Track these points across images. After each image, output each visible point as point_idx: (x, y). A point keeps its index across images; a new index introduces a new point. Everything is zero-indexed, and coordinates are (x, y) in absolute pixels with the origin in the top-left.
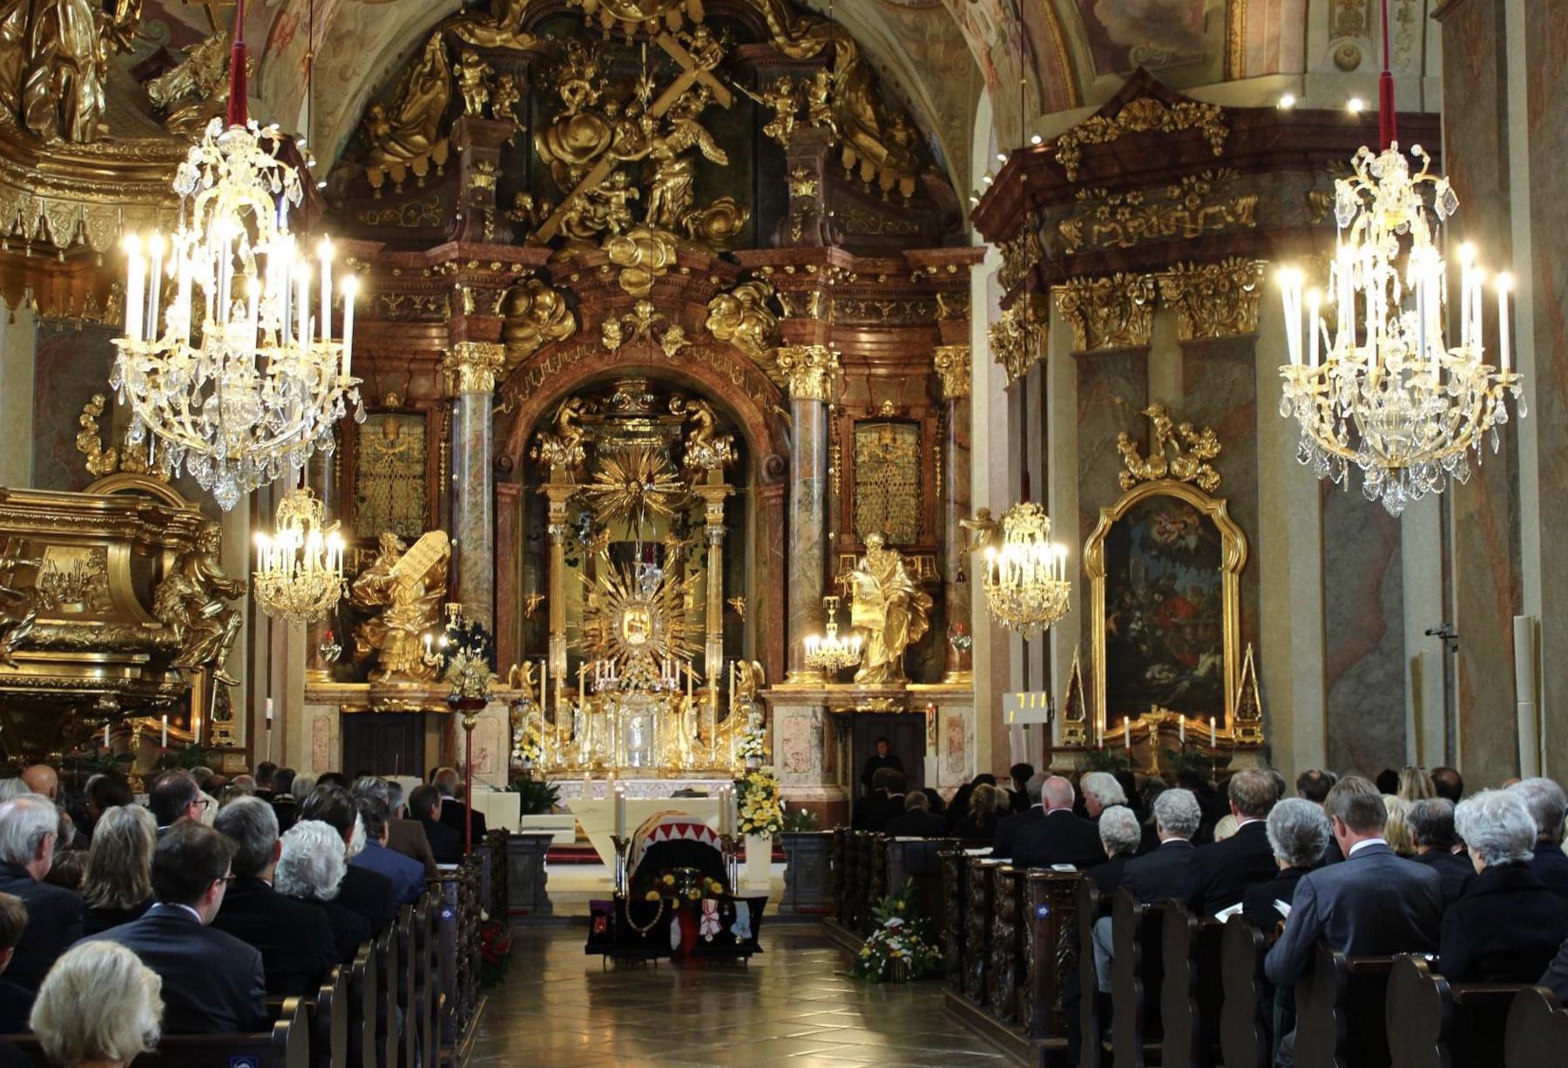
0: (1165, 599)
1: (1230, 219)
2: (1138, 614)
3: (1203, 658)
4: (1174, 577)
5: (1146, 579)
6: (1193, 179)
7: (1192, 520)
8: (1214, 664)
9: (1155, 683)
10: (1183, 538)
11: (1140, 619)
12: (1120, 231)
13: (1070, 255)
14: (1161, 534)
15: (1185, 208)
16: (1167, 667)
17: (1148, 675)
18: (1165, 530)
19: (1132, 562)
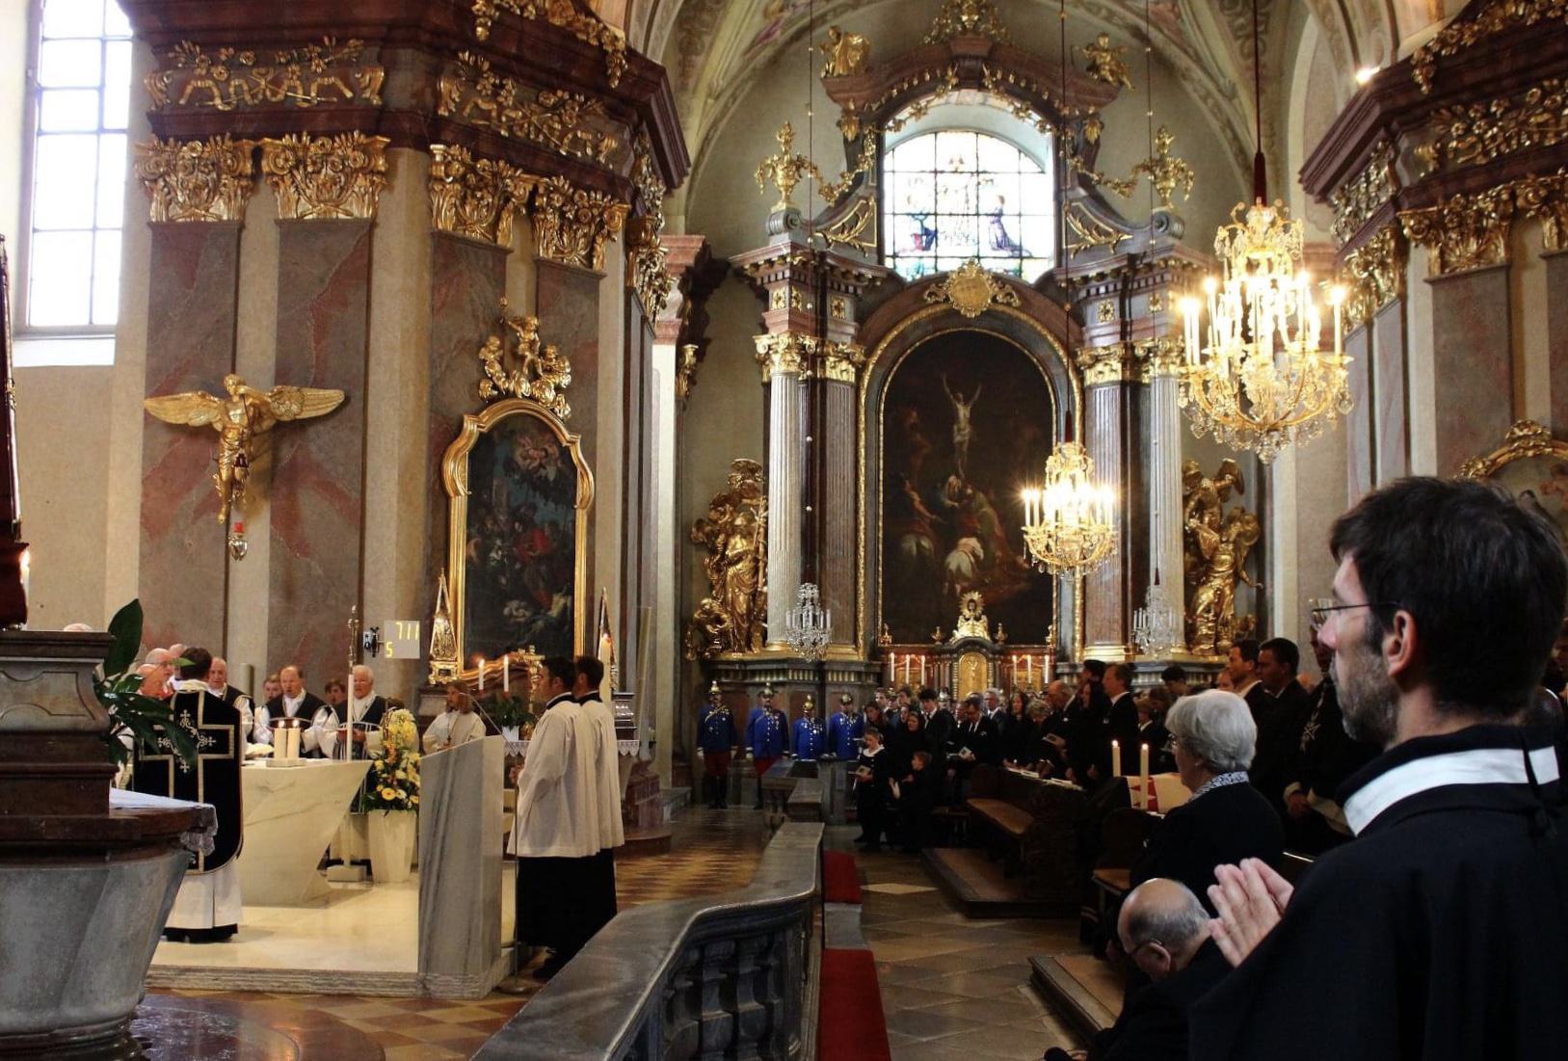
0: (524, 531)
1: (589, 151)
2: (499, 542)
3: (556, 598)
4: (534, 507)
5: (508, 506)
6: (566, 96)
7: (553, 450)
8: (565, 605)
9: (512, 620)
10: (545, 468)
11: (500, 548)
12: (494, 114)
13: (443, 117)
14: (525, 459)
15: (561, 122)
16: (523, 604)
17: (506, 611)
18: (526, 453)
19: (495, 483)
